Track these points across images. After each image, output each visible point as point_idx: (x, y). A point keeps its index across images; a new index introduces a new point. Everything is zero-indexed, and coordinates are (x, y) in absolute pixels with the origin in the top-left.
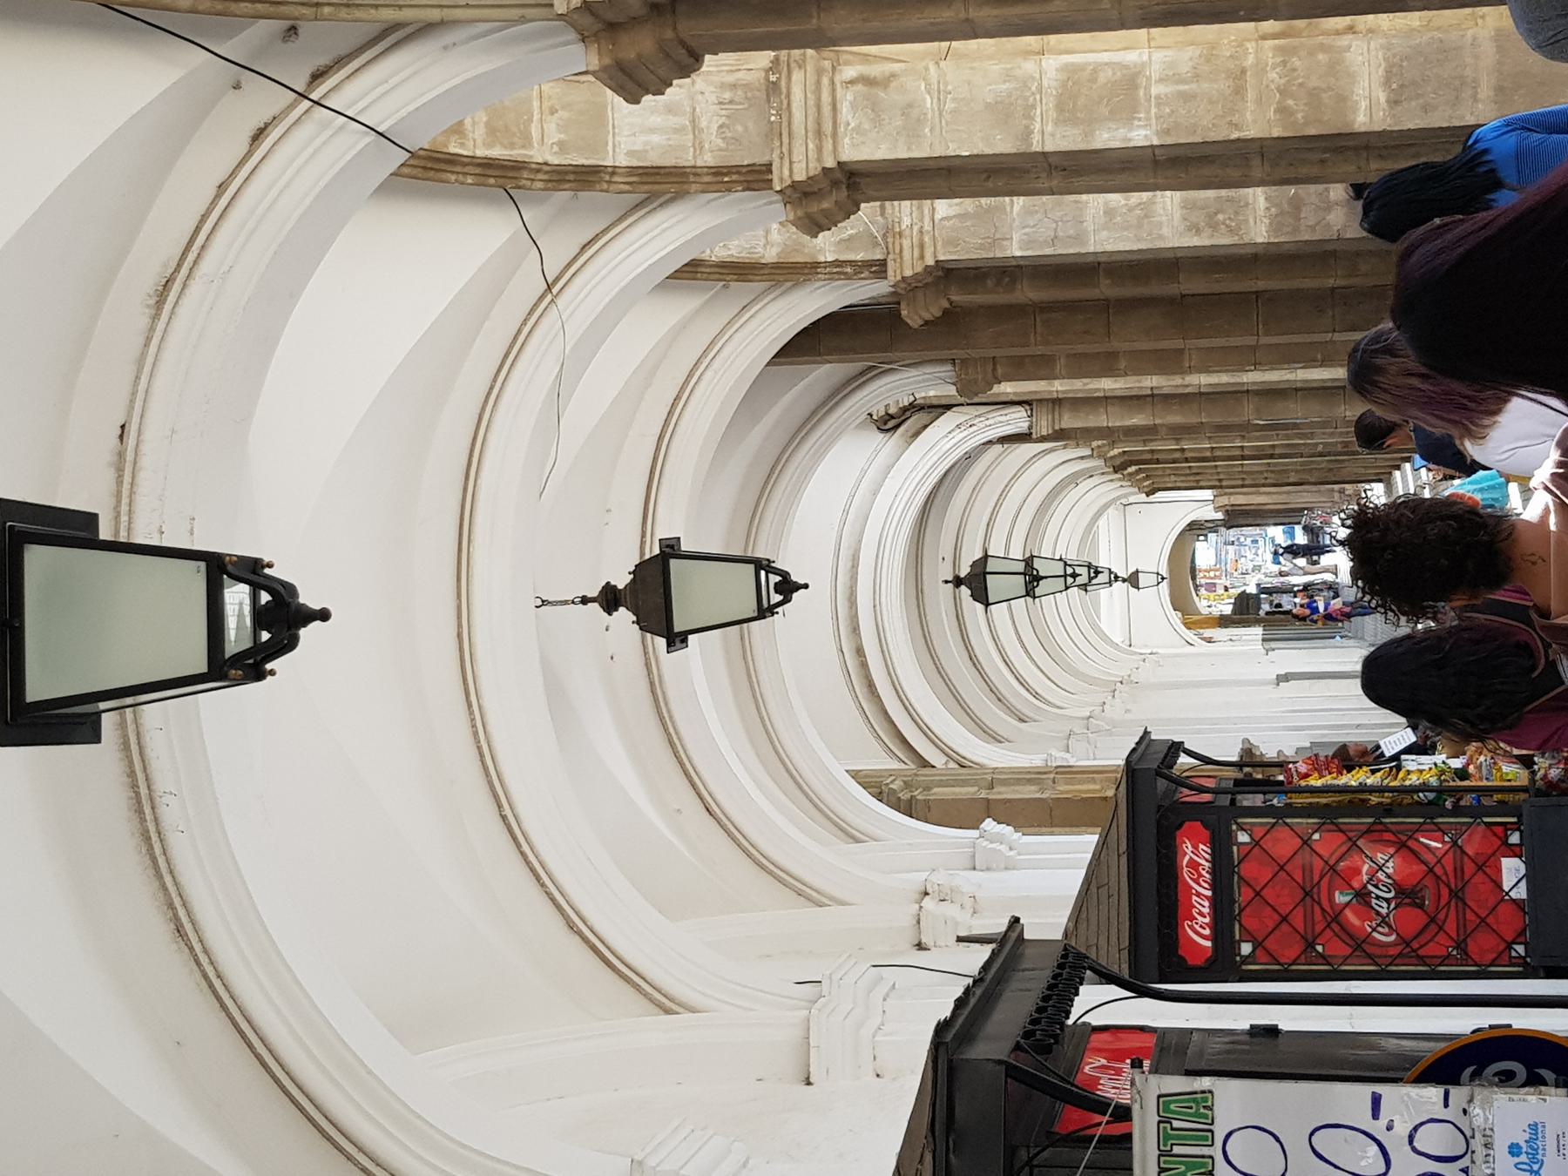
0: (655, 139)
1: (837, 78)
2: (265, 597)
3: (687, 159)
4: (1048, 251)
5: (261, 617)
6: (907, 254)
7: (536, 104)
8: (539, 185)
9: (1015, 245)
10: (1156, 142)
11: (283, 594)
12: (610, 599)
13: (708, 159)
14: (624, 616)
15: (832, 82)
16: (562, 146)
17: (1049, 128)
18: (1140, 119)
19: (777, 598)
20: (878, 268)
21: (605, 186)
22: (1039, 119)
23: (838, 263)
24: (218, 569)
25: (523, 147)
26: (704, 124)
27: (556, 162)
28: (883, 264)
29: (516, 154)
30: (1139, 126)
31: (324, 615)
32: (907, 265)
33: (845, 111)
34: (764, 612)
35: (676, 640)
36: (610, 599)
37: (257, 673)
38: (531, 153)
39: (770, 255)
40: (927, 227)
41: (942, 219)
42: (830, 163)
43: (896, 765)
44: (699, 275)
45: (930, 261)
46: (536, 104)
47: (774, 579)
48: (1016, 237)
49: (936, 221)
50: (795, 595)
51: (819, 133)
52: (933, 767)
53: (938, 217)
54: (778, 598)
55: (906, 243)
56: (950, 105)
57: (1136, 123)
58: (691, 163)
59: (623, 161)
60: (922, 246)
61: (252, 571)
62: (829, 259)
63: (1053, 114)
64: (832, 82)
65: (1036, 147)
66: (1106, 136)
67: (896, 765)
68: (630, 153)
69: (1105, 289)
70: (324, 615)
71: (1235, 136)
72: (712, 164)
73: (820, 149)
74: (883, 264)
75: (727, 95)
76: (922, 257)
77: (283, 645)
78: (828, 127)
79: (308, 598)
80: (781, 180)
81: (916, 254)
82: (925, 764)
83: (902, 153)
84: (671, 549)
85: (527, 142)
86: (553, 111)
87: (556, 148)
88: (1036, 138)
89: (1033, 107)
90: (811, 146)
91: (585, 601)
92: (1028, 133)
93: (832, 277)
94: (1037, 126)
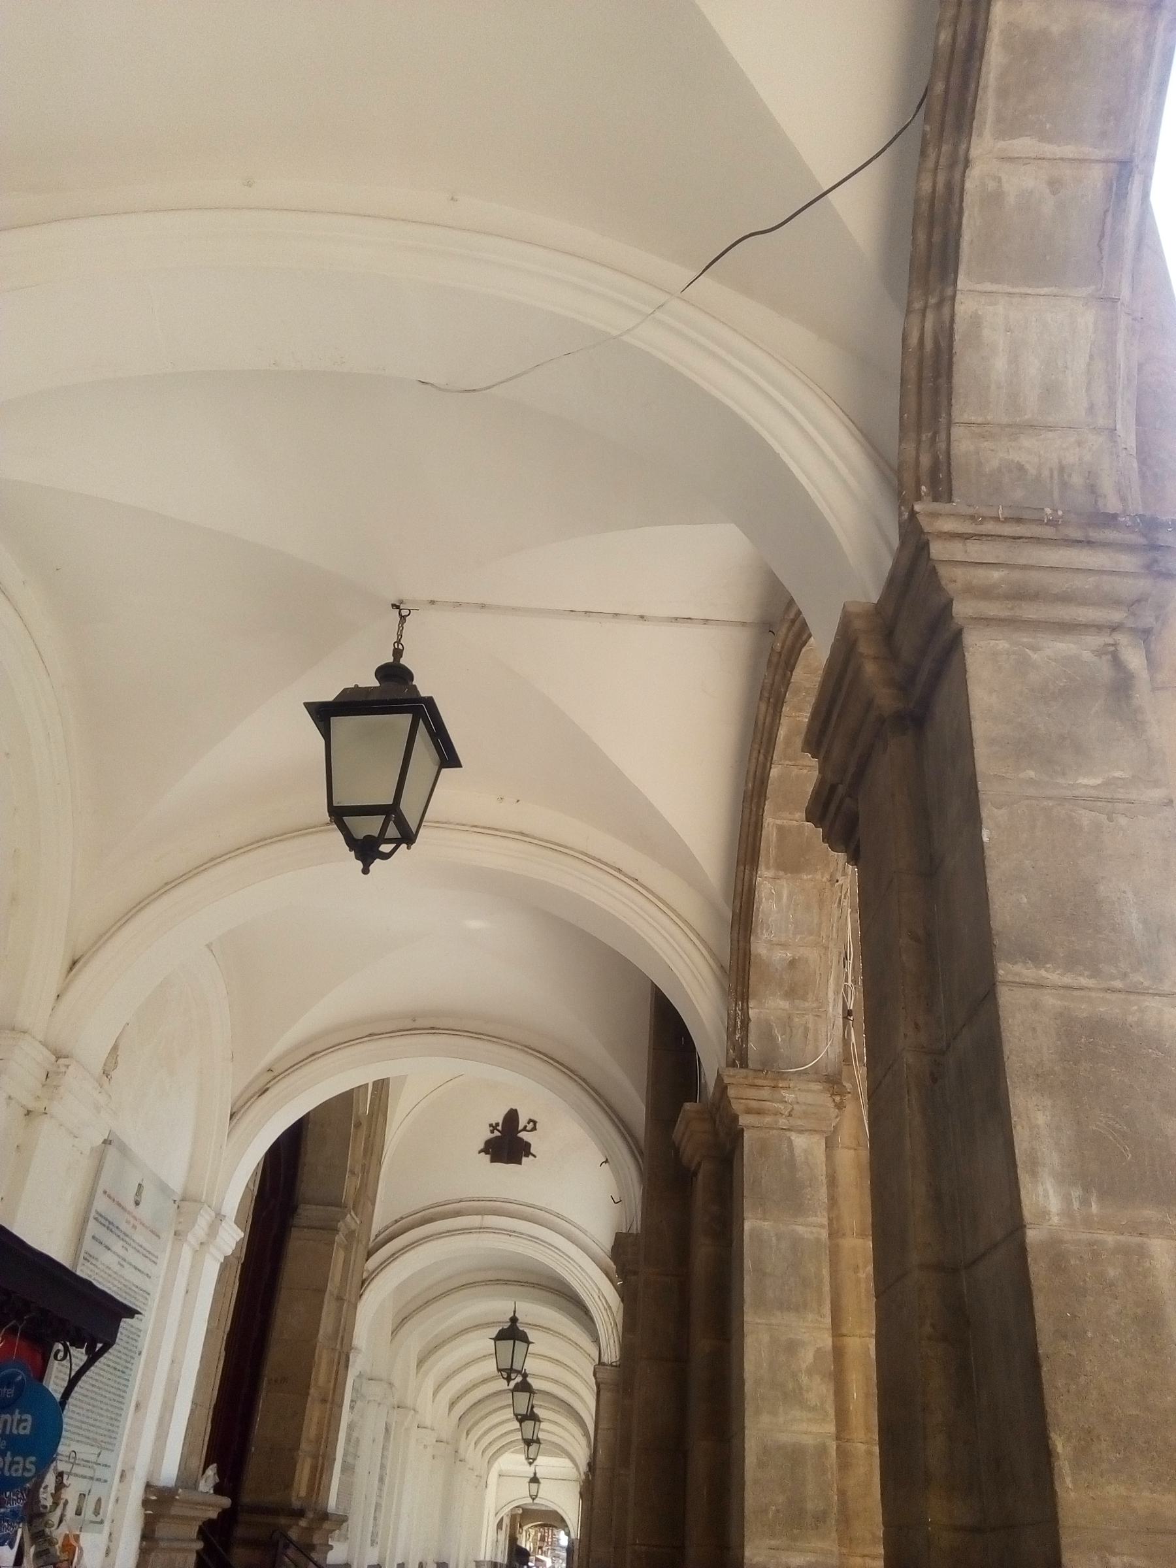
0: (1000, 364)
1: (1122, 639)
3: (964, 411)
4: (748, 1263)
6: (752, 1093)
7: (1069, 150)
8: (926, 186)
9: (759, 1223)
10: (1033, 1235)
13: (963, 444)
15: (1114, 628)
16: (994, 199)
17: (1050, 1001)
18: (1085, 1202)
20: (739, 1058)
21: (918, 305)
22: (1067, 980)
23: (746, 1021)
25: (999, 119)
26: (1026, 442)
27: (968, 185)
28: (744, 1064)
29: (988, 104)
30: (1067, 1199)
32: (740, 1097)
33: (1064, 646)
38: (987, 133)
39: (759, 947)
40: (782, 1122)
41: (790, 1141)
42: (962, 609)
43: (374, 1232)
44: (742, 868)
45: (744, 1120)
46: (1069, 150)
48: (766, 1225)
49: (788, 1134)
51: (1019, 595)
52: (367, 1260)
53: (794, 1136)
55: (765, 1093)
56: (1085, 817)
57: (1076, 1193)
58: (957, 416)
59: (965, 306)
60: (759, 1112)
62: (750, 1011)
63: (1083, 1010)
64: (1114, 628)
65: (1005, 970)
66: (1041, 1119)
67: (374, 1232)
68: (976, 322)
69: (702, 1345)
71: (1060, 1445)
72: (954, 451)
73: (986, 593)
74: (744, 1064)
75: (1077, 480)
76: (749, 1111)
78: (1030, 611)
80: (935, 515)
81: (753, 1104)
82: (369, 1255)
83: (981, 729)
85: (1009, 128)
86: (1054, 184)
87: (991, 185)
88: (1027, 972)
89: (1095, 973)
90: (996, 575)
92: (1034, 955)
93: (732, 1018)
94: (1052, 976)
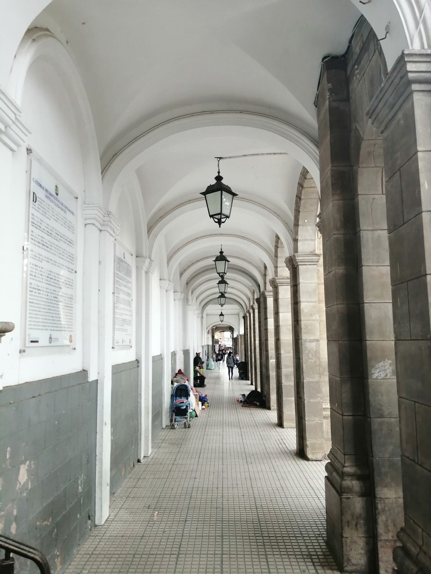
12: (221, 252)
19: (221, 275)
31: (220, 227)
35: (215, 261)
36: (221, 252)
54: (221, 275)
70: (220, 227)
79: (222, 225)
91: (221, 249)
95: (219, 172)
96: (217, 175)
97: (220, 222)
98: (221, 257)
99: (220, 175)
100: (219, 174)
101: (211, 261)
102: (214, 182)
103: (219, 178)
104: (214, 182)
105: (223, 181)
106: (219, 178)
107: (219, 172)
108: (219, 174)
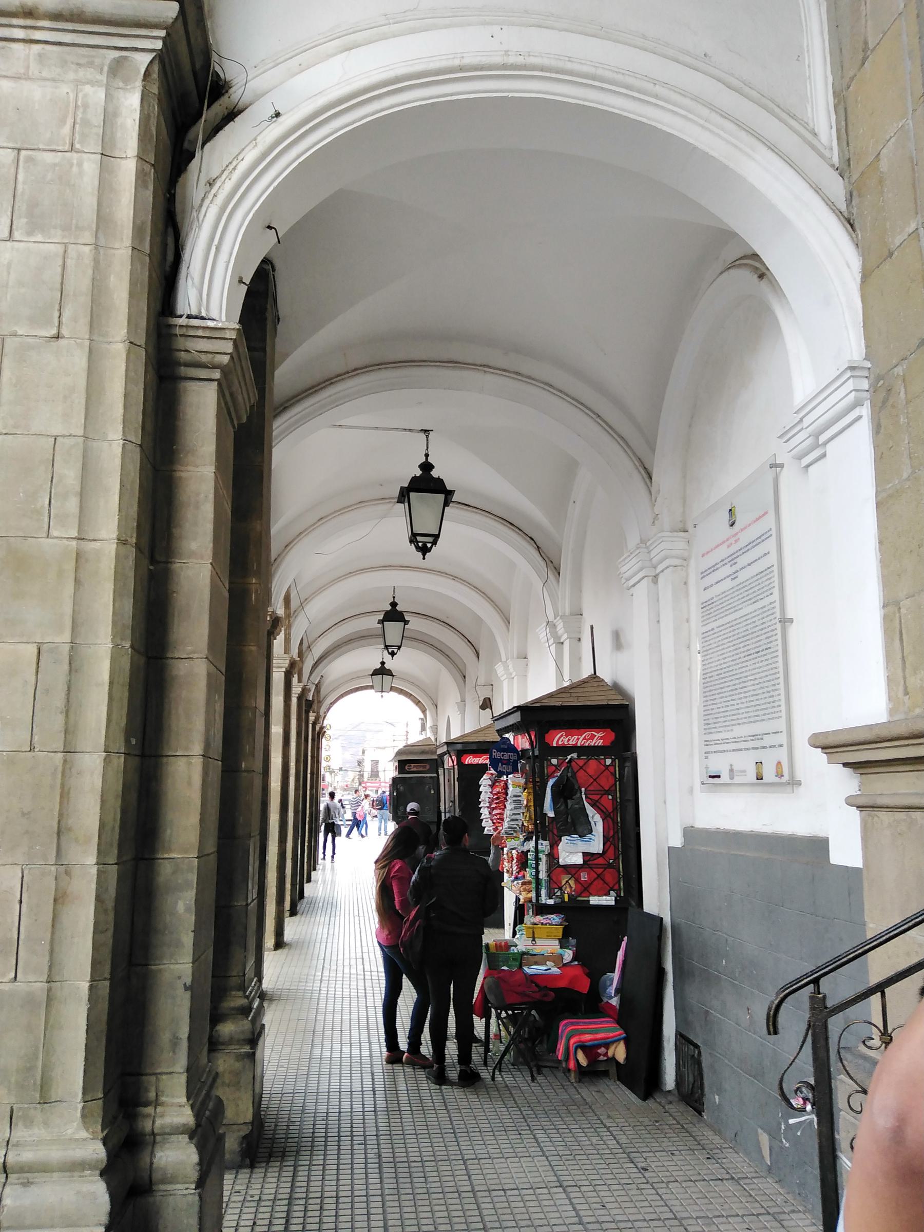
2: (429, 545)
5: (425, 544)
11: (429, 550)
12: (394, 604)
14: (389, 608)
19: (390, 650)
24: (436, 537)
34: (387, 647)
35: (381, 622)
36: (394, 604)
37: (411, 542)
47: (395, 651)
50: (390, 656)
61: (434, 543)
77: (417, 548)
84: (406, 622)
91: (394, 597)
95: (427, 455)
96: (424, 460)
97: (424, 550)
98: (394, 615)
99: (430, 460)
100: (427, 459)
101: (372, 623)
102: (419, 473)
103: (427, 467)
104: (419, 473)
105: (435, 473)
106: (427, 467)
107: (427, 455)
108: (427, 459)
